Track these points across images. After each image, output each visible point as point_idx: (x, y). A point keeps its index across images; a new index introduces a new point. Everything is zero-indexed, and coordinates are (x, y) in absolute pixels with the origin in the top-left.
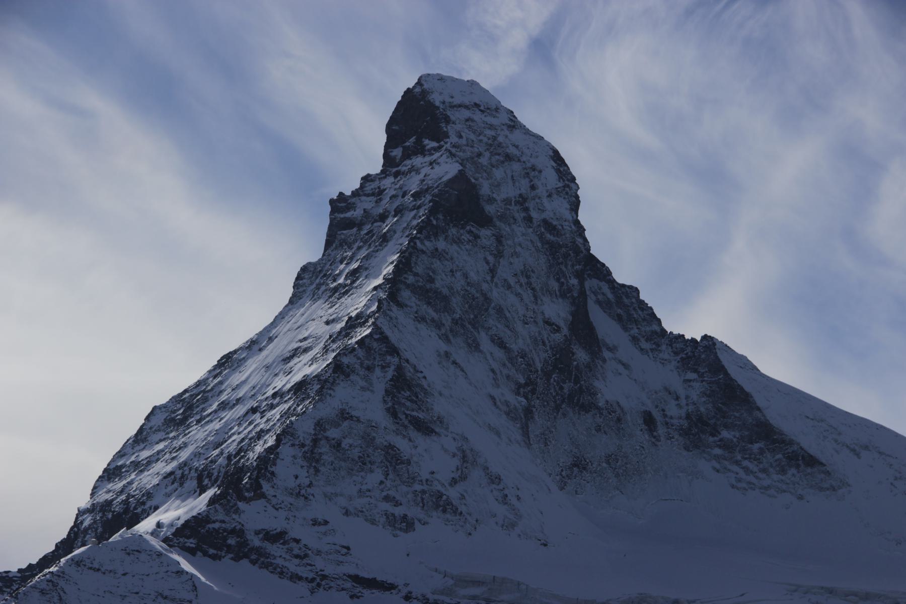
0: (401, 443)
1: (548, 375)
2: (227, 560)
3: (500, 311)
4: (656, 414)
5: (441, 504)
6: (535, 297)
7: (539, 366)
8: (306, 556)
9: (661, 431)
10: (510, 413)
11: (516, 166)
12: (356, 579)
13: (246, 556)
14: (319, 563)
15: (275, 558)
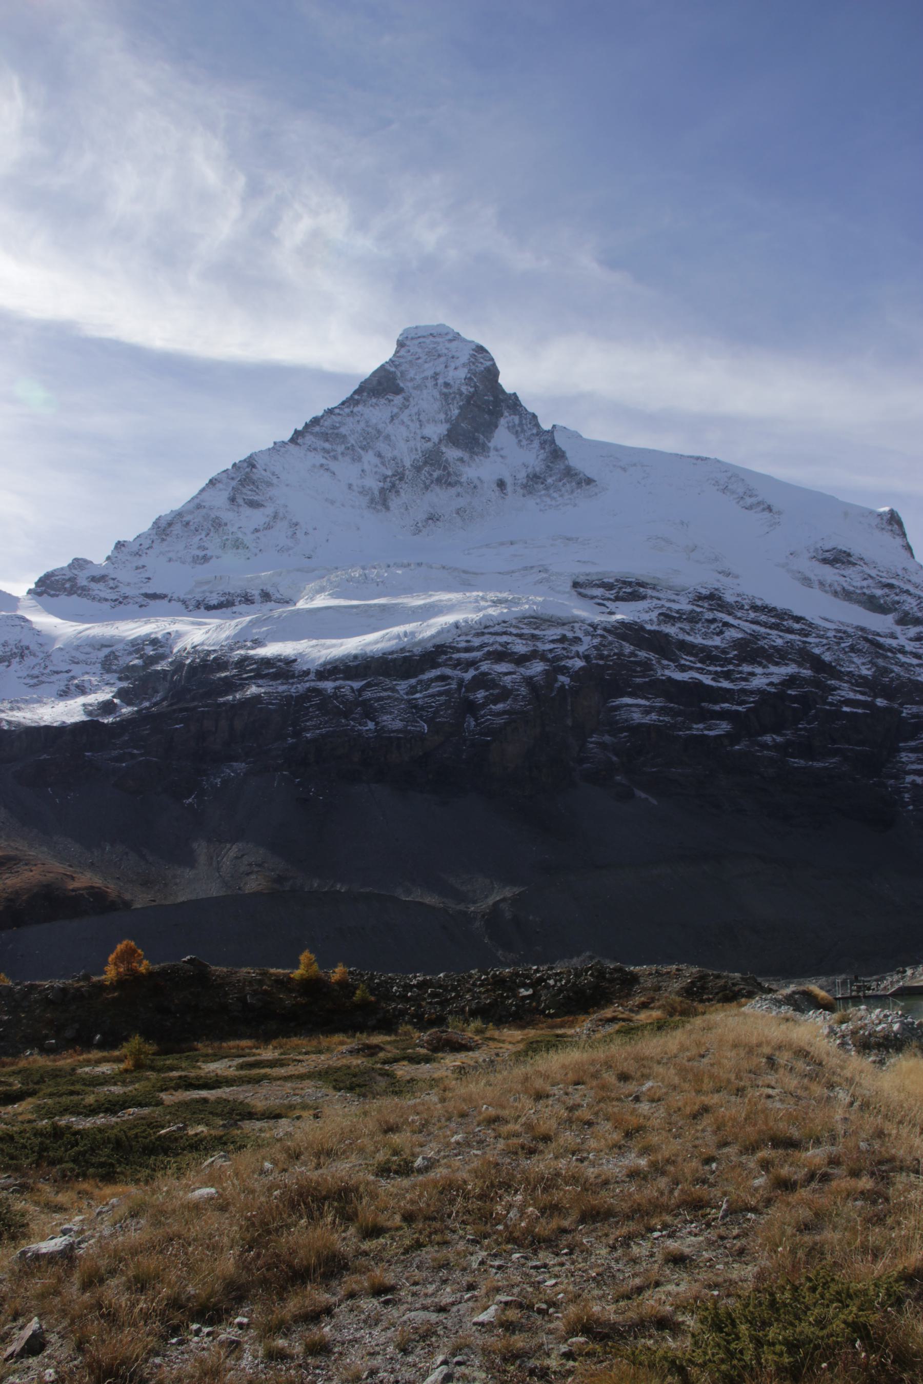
0: (227, 516)
1: (418, 469)
2: (63, 598)
3: (388, 437)
4: (509, 481)
5: (238, 544)
6: (421, 426)
7: (408, 464)
8: (117, 587)
9: (509, 488)
10: (364, 491)
11: (443, 359)
12: (147, 596)
13: (75, 593)
14: (125, 590)
15: (93, 590)
